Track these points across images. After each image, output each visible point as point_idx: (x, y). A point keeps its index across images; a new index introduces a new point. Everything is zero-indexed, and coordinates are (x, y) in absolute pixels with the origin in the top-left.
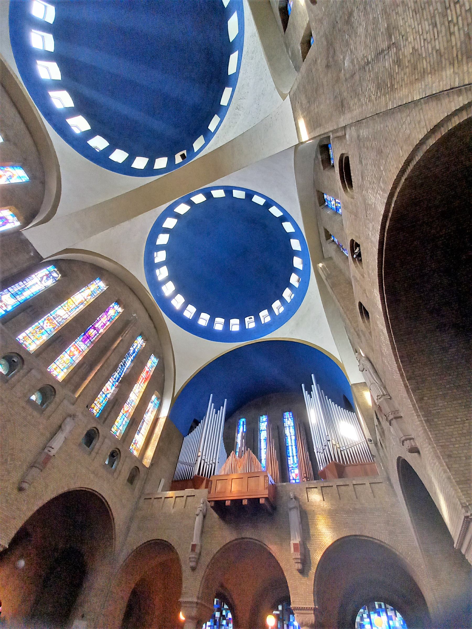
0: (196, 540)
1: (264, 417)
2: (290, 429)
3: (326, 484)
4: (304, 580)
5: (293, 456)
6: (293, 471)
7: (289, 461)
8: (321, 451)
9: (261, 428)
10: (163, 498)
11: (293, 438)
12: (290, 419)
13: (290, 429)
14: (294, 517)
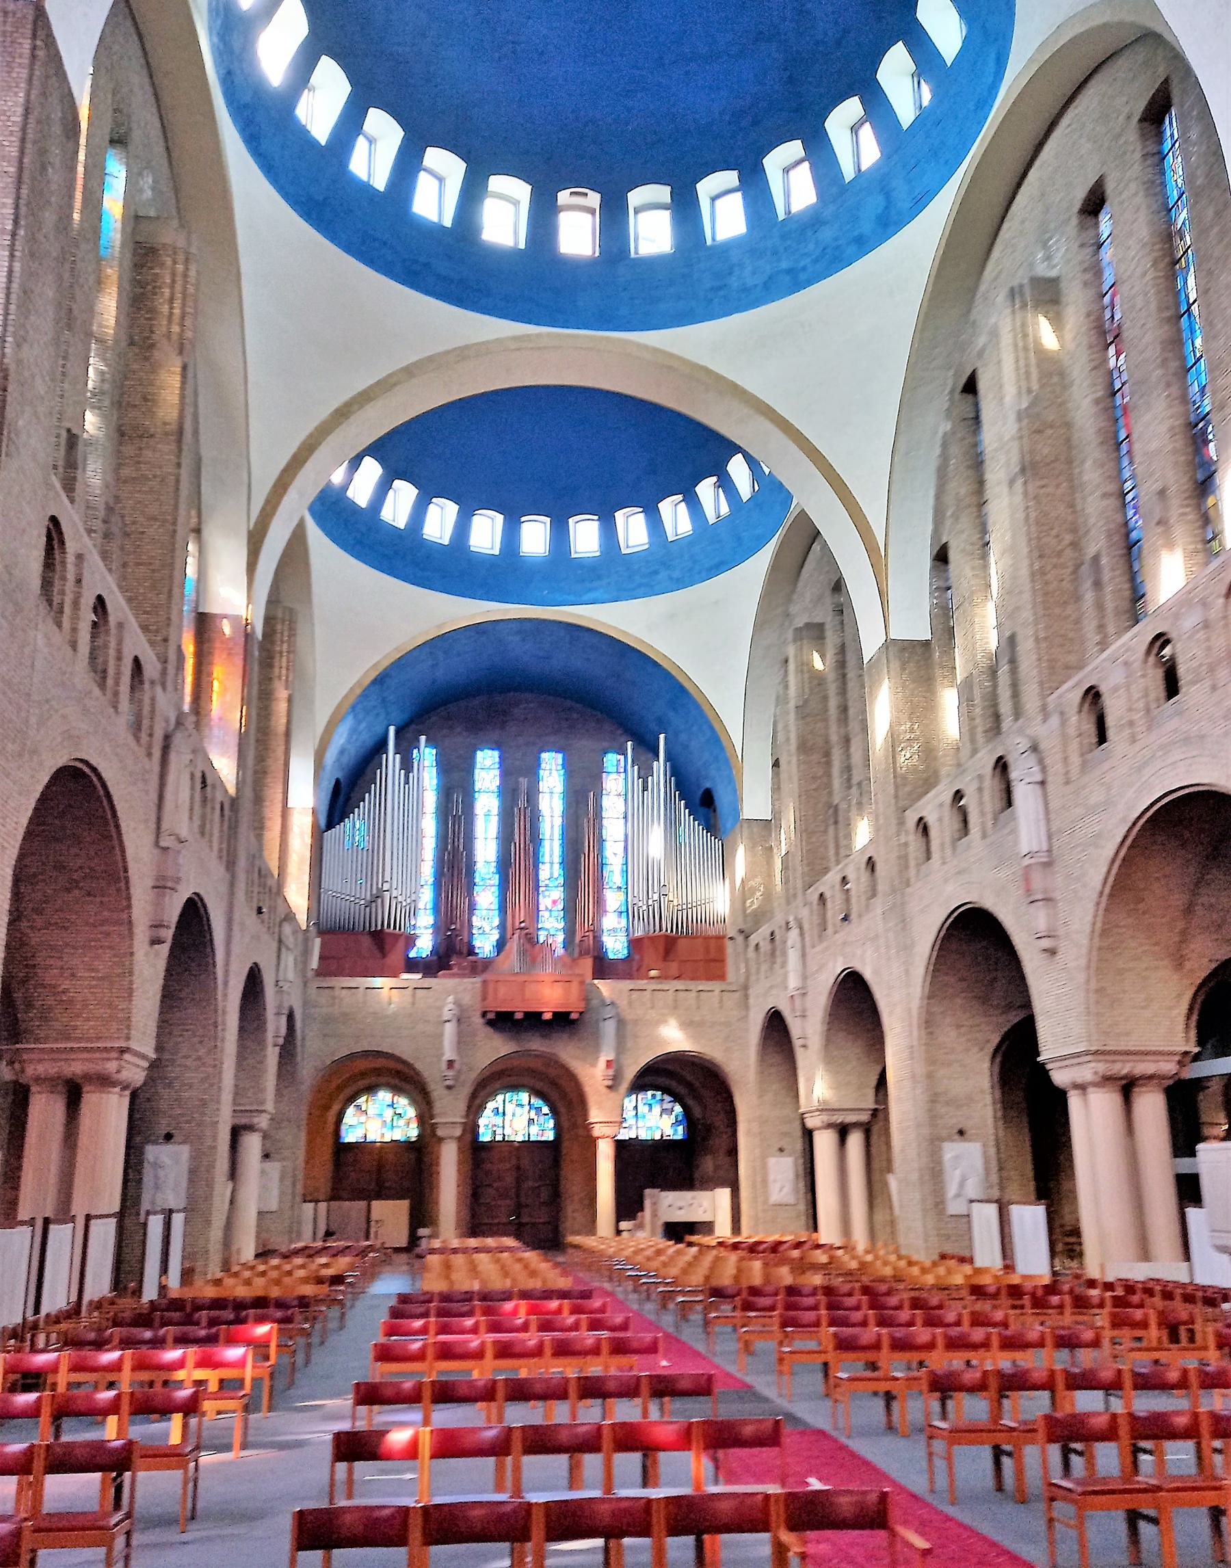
0: (449, 1053)
1: (488, 753)
2: (551, 798)
3: (659, 987)
4: (612, 1095)
5: (552, 863)
6: (547, 893)
7: (541, 872)
8: (645, 907)
9: (477, 786)
10: (361, 990)
11: (558, 821)
12: (554, 773)
13: (551, 798)
14: (609, 1028)
